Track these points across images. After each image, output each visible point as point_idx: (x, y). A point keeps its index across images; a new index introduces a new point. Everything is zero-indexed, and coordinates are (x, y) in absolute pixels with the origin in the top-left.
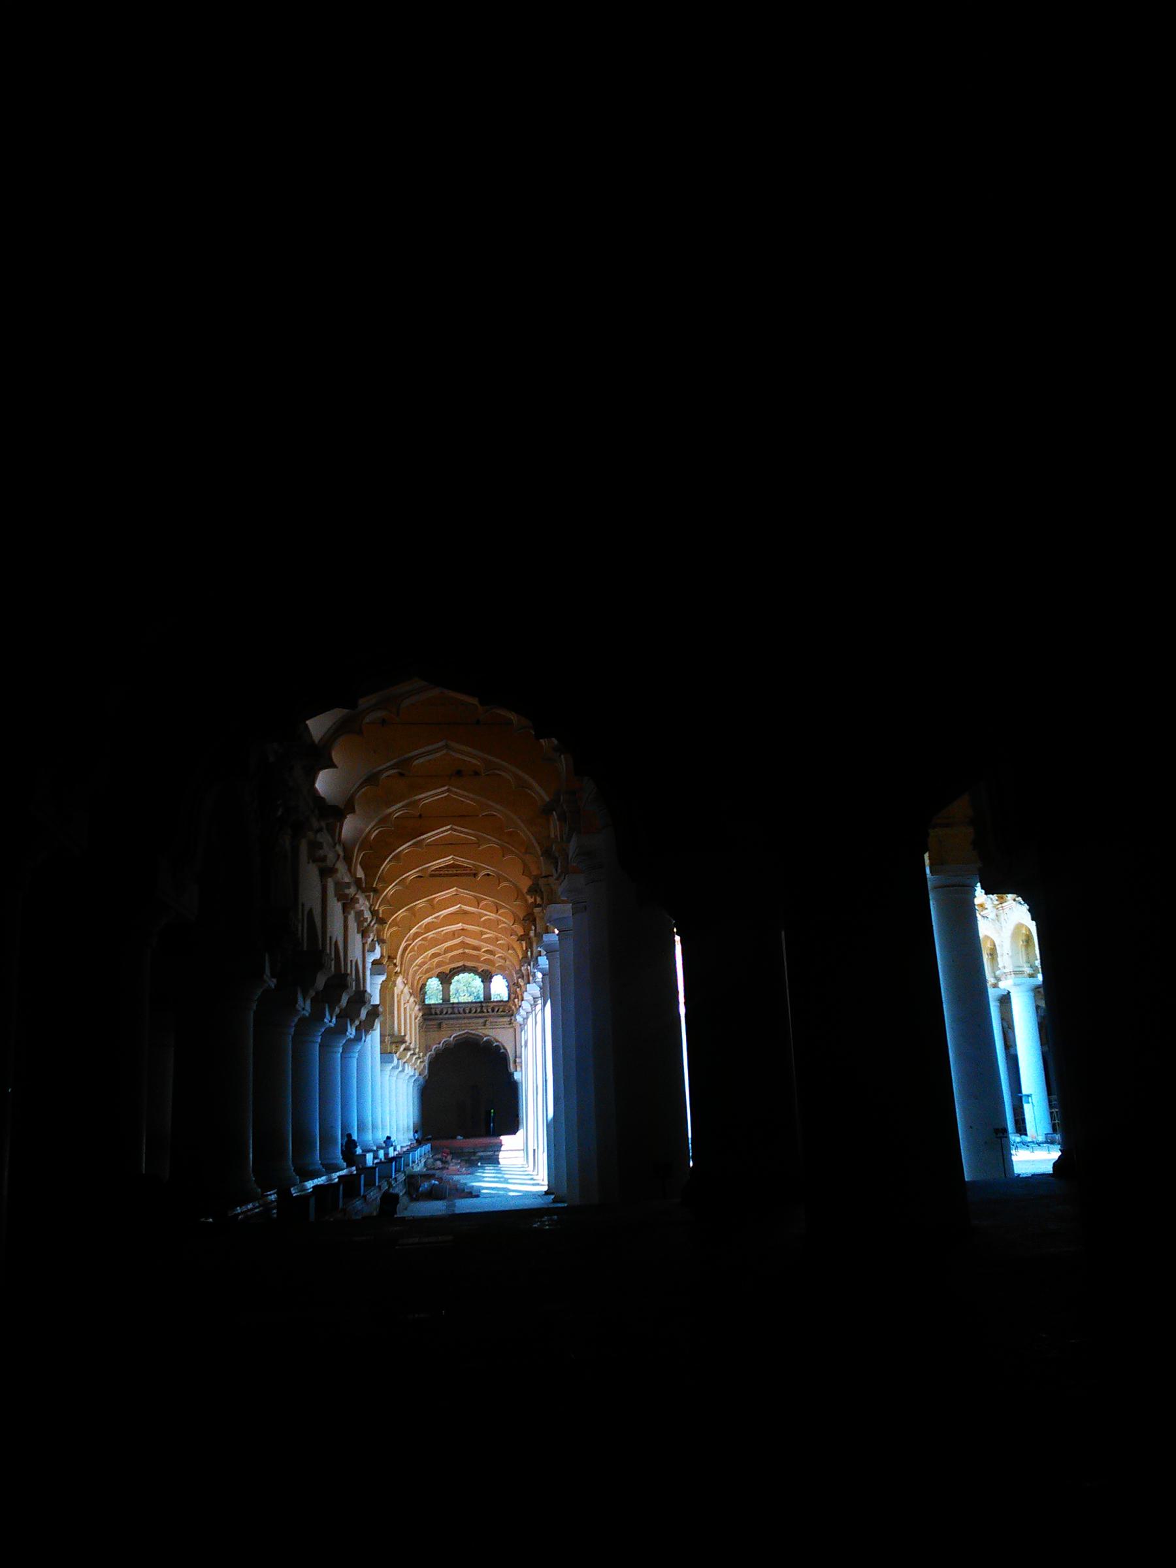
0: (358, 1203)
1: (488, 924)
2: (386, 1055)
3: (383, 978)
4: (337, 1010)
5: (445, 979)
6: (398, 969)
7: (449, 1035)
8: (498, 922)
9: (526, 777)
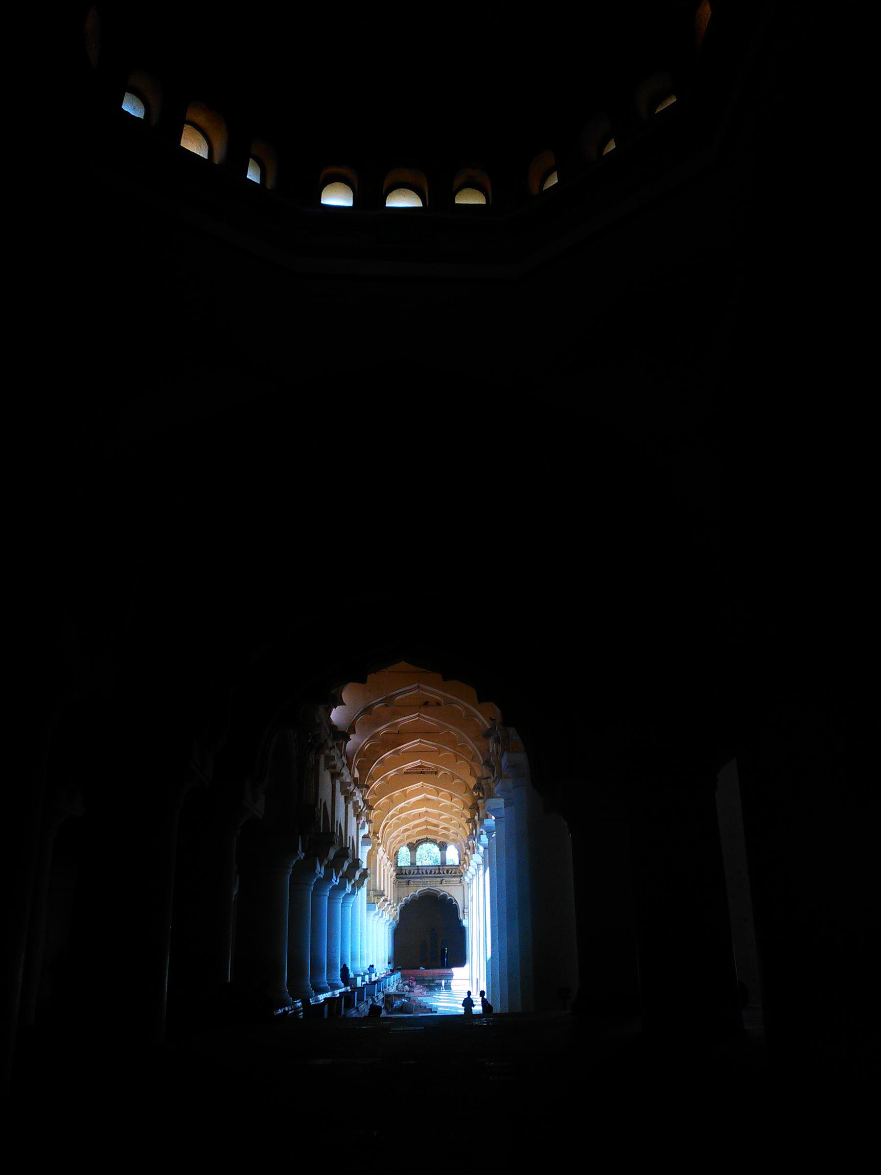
1: (446, 808)
2: (370, 904)
3: (370, 848)
4: (341, 873)
5: (413, 848)
6: (380, 841)
7: (415, 890)
8: (452, 807)
9: (475, 710)
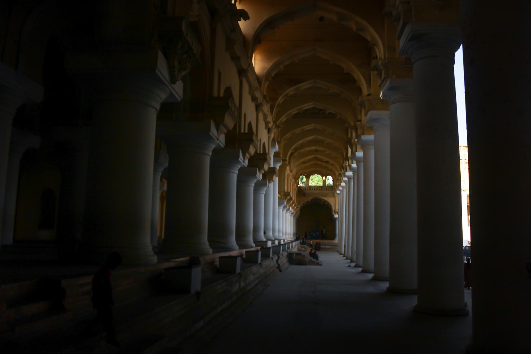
0: (255, 269)
4: (247, 155)
6: (287, 162)
